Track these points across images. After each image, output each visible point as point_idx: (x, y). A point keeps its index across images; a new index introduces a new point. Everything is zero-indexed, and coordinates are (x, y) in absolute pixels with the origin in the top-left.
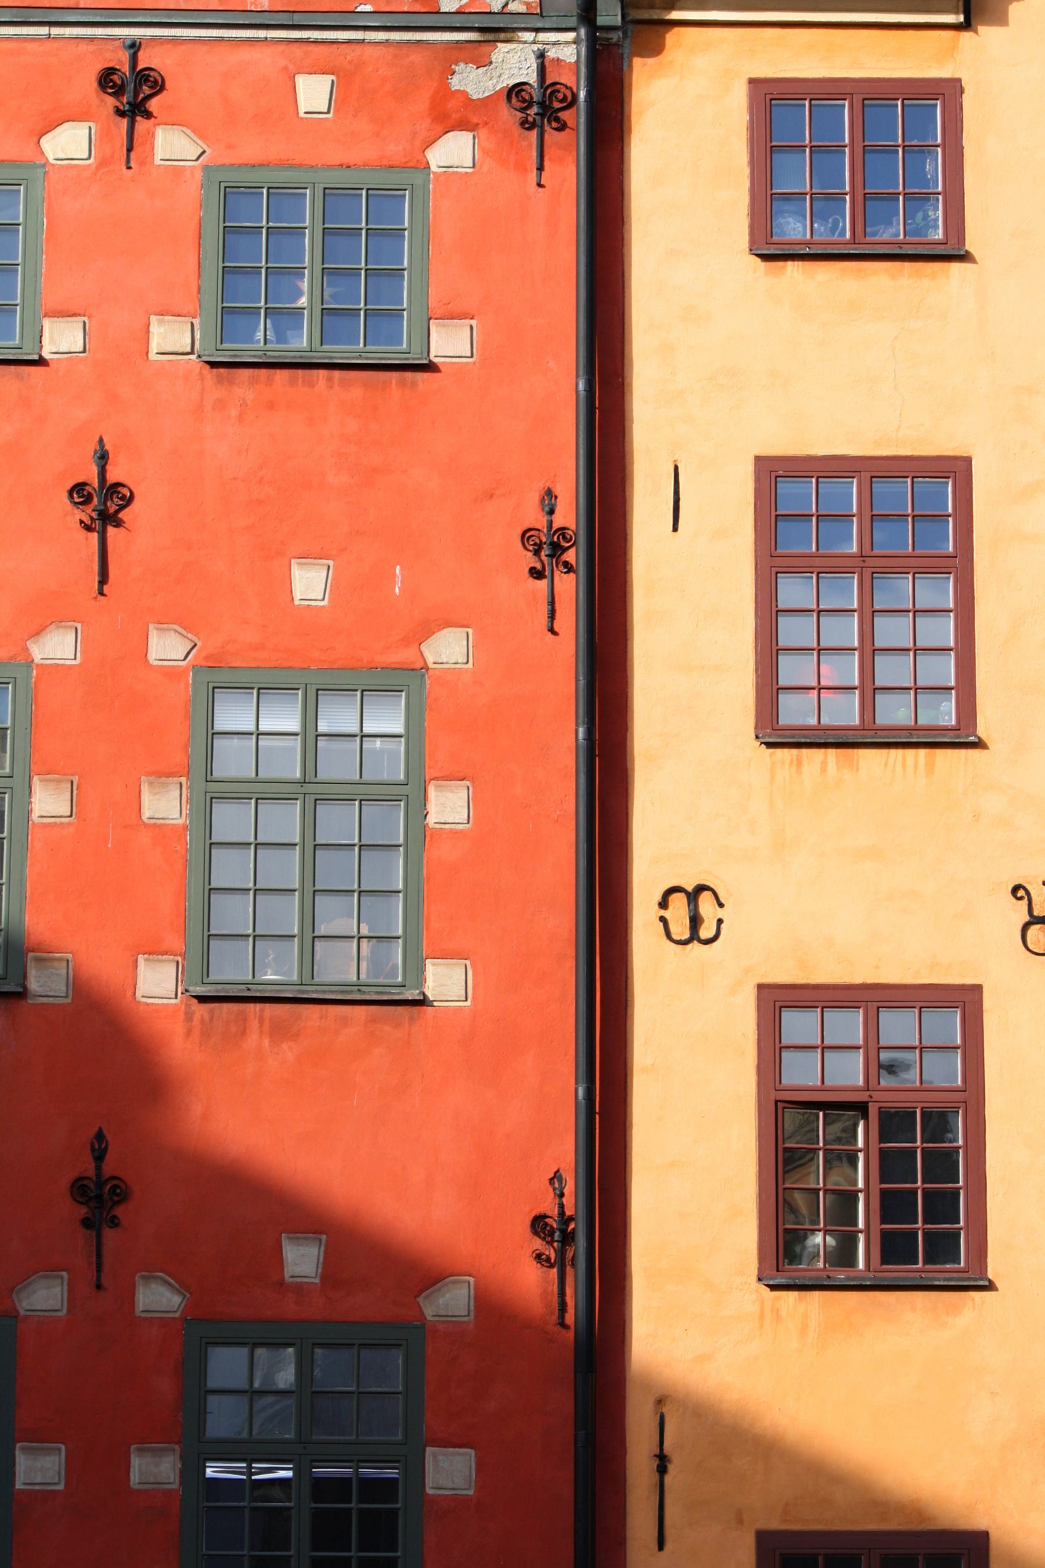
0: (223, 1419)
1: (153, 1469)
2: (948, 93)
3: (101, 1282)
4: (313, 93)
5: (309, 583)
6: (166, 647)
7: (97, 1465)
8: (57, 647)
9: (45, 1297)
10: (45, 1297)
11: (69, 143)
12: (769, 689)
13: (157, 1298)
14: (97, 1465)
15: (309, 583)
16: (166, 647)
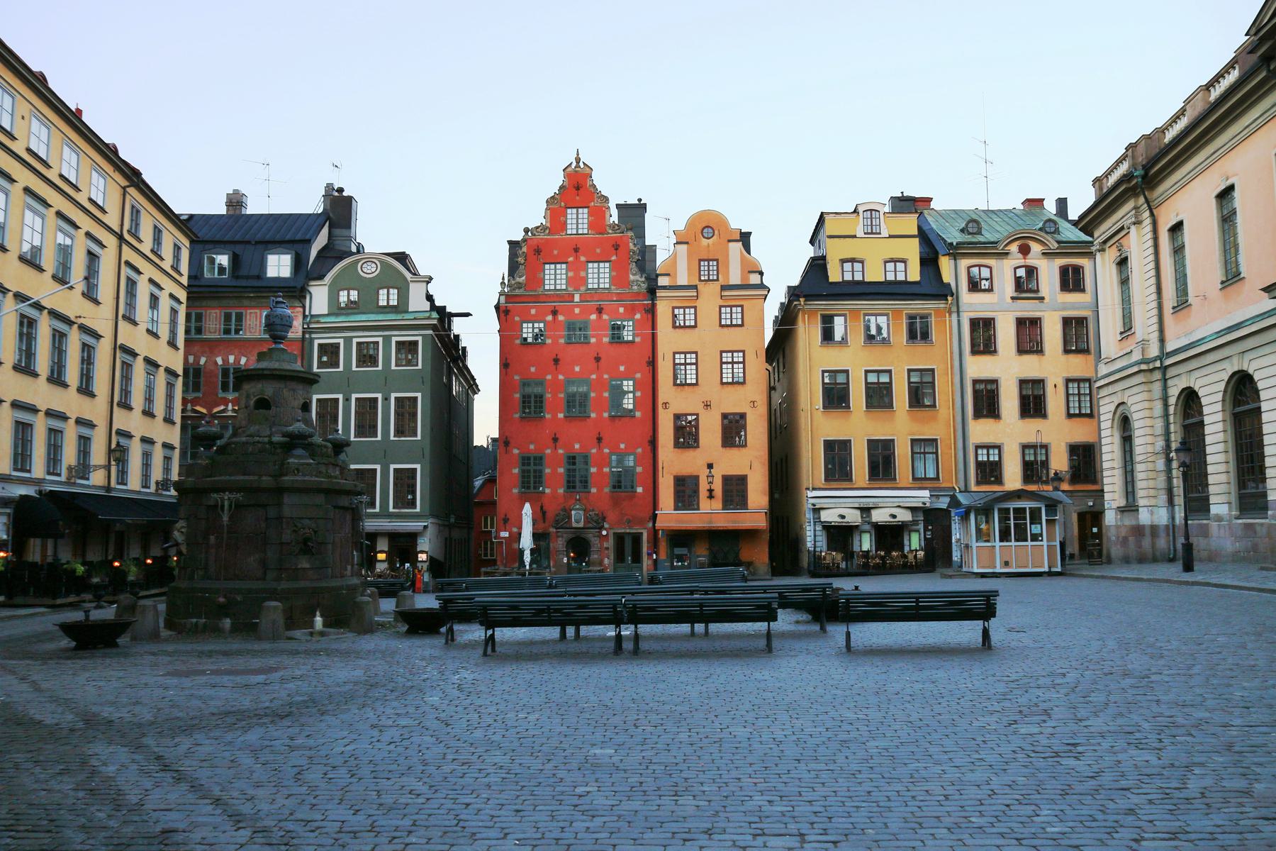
0: (614, 464)
1: (606, 470)
2: (695, 308)
3: (600, 449)
4: (621, 310)
5: (622, 368)
6: (606, 376)
7: (600, 469)
8: (594, 376)
9: (594, 451)
10: (594, 451)
11: (593, 317)
12: (675, 378)
13: (606, 451)
14: (600, 469)
15: (622, 368)
16: (606, 376)
